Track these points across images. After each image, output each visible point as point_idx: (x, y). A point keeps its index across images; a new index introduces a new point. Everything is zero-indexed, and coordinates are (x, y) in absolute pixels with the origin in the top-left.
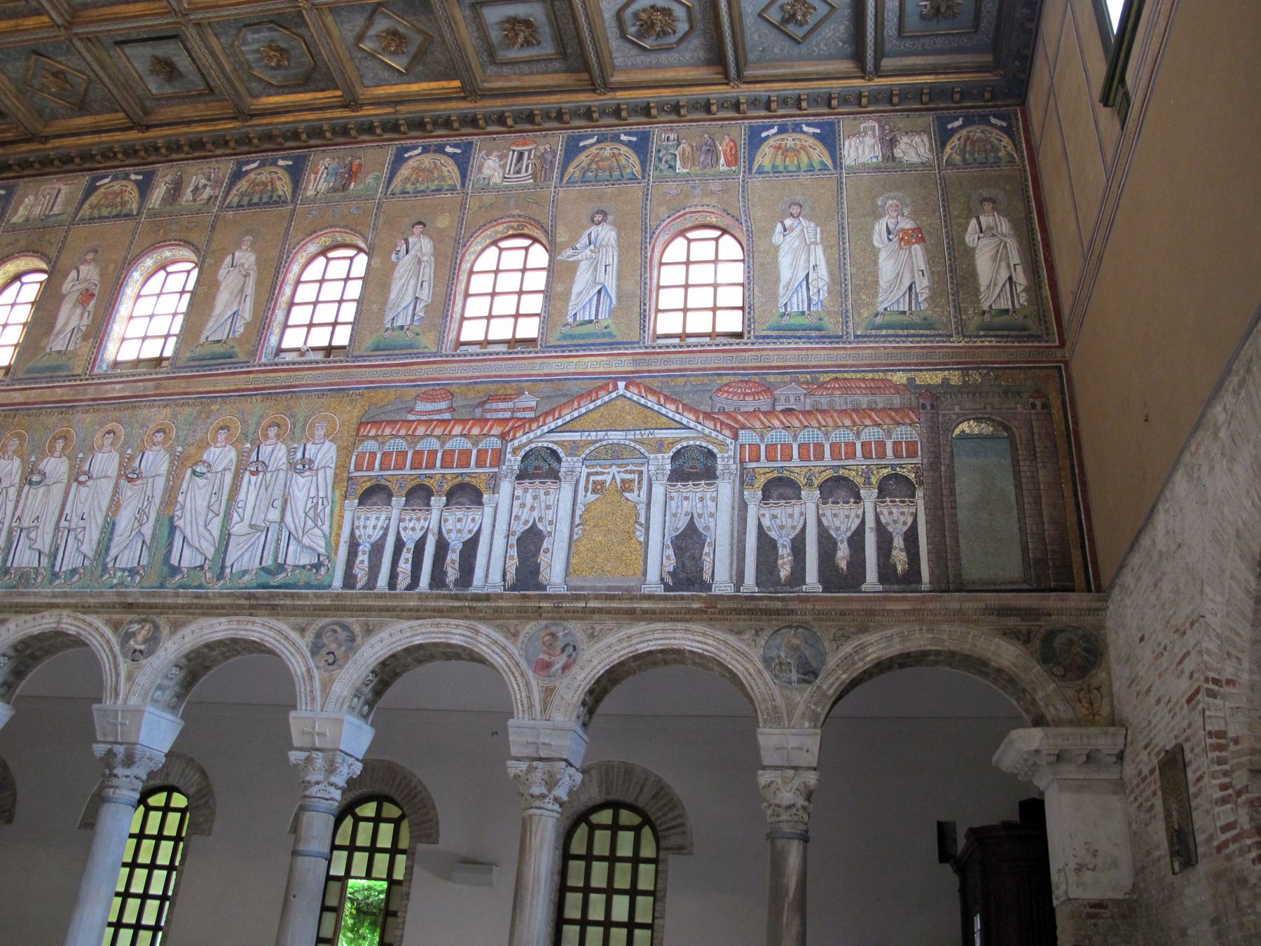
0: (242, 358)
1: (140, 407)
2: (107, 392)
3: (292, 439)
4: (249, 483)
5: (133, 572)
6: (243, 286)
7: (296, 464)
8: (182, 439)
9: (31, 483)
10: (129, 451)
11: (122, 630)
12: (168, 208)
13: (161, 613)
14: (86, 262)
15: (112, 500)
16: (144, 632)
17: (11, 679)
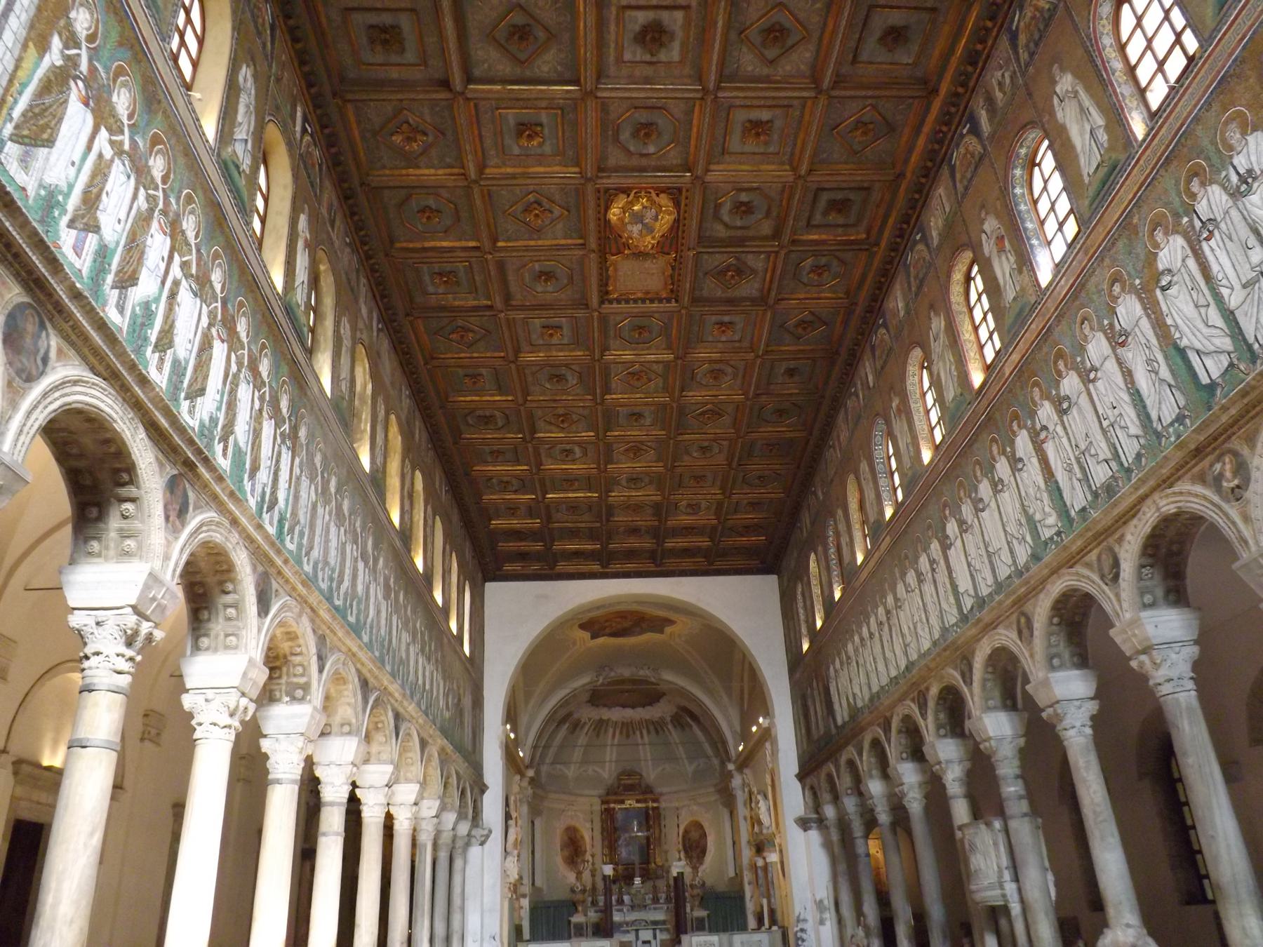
0: (1122, 157)
1: (1087, 281)
2: (1059, 294)
3: (1219, 172)
4: (1212, 250)
5: (1180, 419)
6: (1080, 105)
7: (1239, 187)
8: (1133, 272)
9: (1065, 412)
10: (1106, 322)
11: (1209, 478)
12: (996, 120)
13: (1229, 437)
14: (982, 222)
15: (1123, 372)
16: (1228, 467)
17: (1171, 583)
